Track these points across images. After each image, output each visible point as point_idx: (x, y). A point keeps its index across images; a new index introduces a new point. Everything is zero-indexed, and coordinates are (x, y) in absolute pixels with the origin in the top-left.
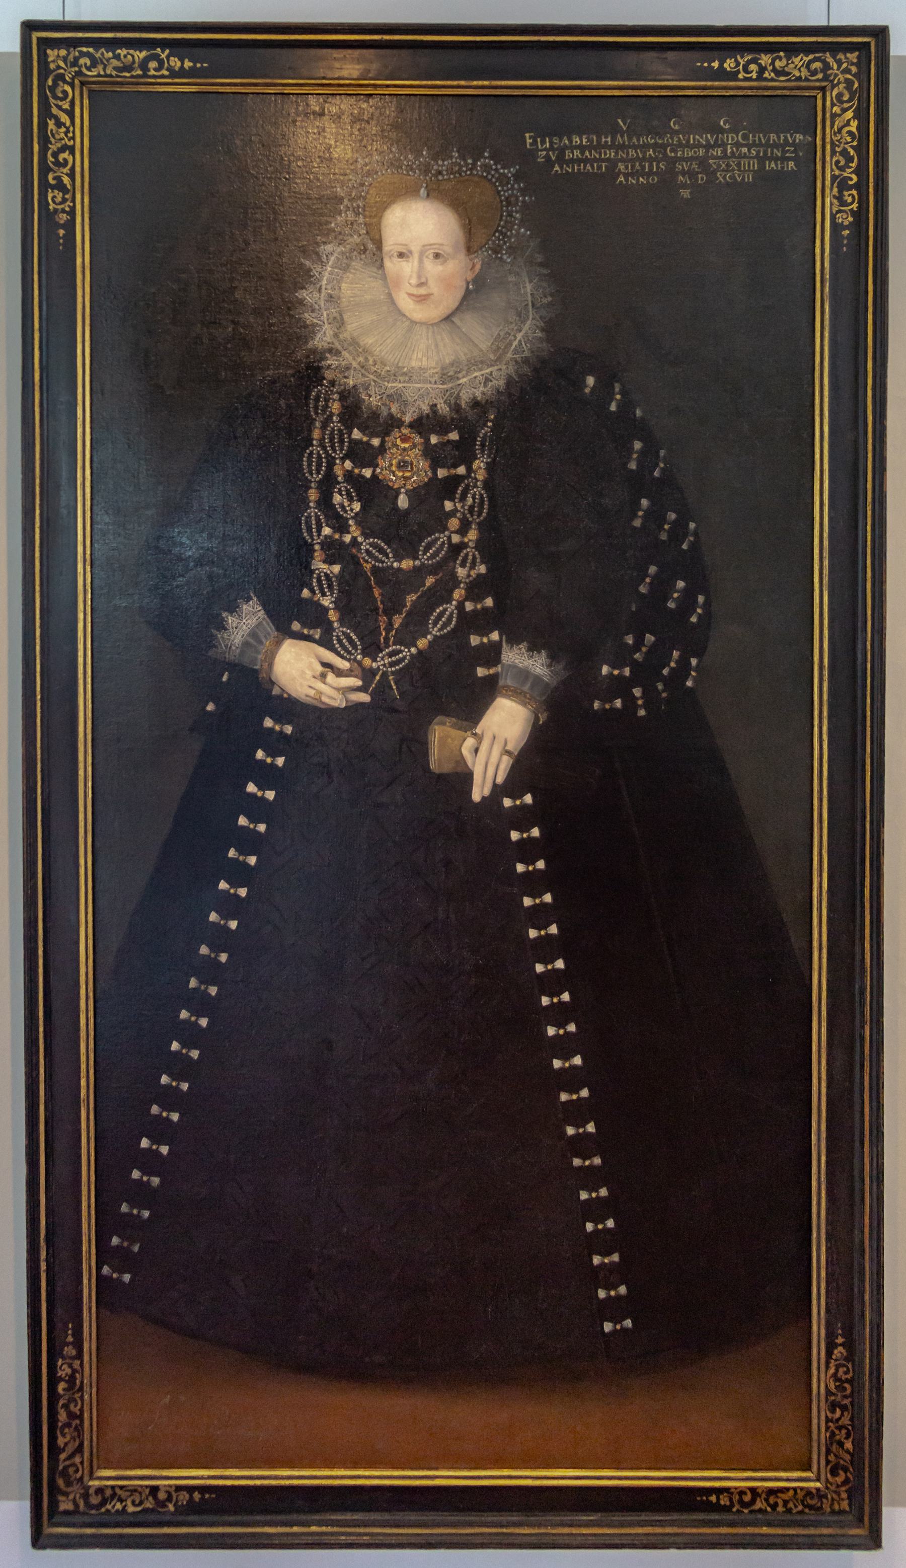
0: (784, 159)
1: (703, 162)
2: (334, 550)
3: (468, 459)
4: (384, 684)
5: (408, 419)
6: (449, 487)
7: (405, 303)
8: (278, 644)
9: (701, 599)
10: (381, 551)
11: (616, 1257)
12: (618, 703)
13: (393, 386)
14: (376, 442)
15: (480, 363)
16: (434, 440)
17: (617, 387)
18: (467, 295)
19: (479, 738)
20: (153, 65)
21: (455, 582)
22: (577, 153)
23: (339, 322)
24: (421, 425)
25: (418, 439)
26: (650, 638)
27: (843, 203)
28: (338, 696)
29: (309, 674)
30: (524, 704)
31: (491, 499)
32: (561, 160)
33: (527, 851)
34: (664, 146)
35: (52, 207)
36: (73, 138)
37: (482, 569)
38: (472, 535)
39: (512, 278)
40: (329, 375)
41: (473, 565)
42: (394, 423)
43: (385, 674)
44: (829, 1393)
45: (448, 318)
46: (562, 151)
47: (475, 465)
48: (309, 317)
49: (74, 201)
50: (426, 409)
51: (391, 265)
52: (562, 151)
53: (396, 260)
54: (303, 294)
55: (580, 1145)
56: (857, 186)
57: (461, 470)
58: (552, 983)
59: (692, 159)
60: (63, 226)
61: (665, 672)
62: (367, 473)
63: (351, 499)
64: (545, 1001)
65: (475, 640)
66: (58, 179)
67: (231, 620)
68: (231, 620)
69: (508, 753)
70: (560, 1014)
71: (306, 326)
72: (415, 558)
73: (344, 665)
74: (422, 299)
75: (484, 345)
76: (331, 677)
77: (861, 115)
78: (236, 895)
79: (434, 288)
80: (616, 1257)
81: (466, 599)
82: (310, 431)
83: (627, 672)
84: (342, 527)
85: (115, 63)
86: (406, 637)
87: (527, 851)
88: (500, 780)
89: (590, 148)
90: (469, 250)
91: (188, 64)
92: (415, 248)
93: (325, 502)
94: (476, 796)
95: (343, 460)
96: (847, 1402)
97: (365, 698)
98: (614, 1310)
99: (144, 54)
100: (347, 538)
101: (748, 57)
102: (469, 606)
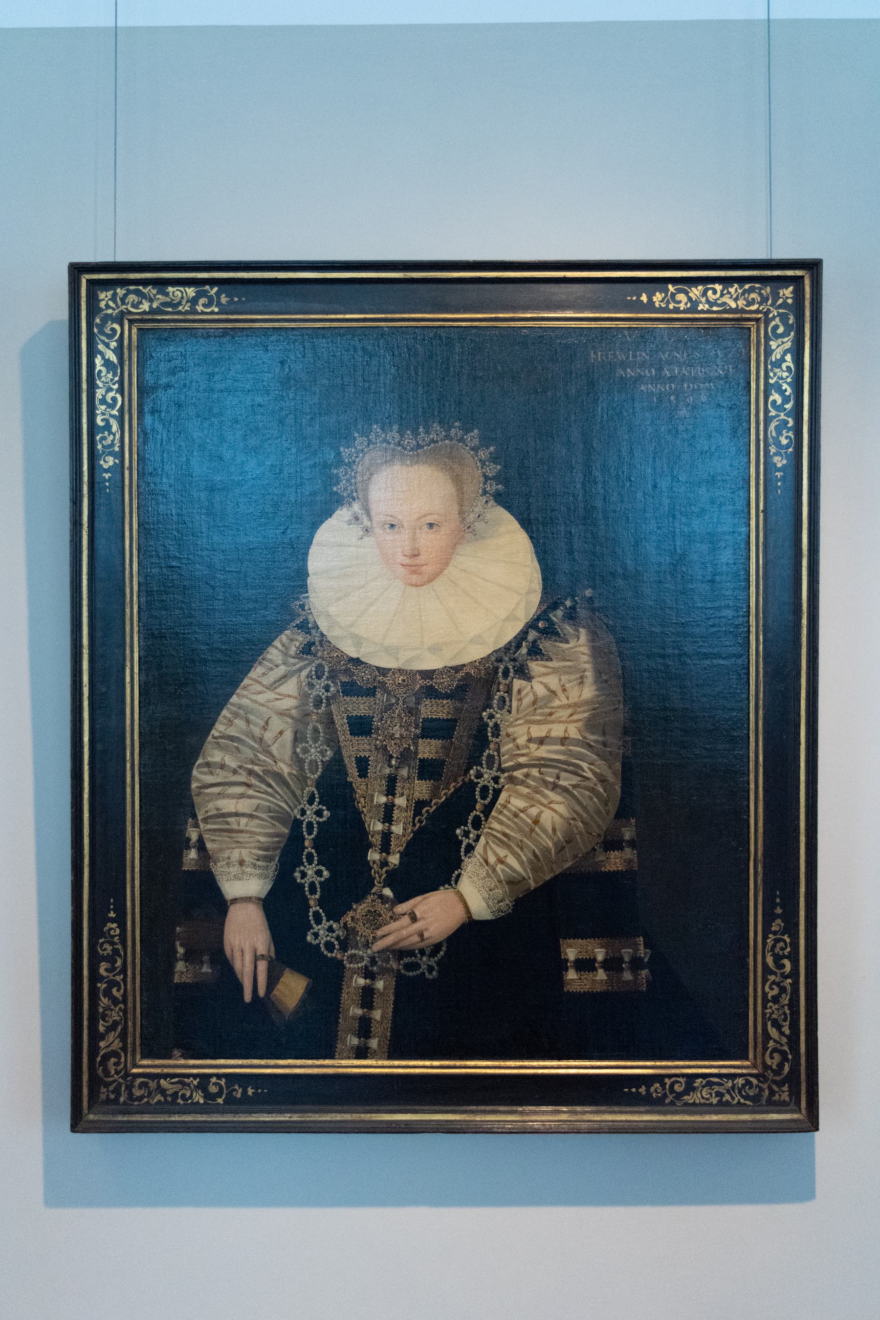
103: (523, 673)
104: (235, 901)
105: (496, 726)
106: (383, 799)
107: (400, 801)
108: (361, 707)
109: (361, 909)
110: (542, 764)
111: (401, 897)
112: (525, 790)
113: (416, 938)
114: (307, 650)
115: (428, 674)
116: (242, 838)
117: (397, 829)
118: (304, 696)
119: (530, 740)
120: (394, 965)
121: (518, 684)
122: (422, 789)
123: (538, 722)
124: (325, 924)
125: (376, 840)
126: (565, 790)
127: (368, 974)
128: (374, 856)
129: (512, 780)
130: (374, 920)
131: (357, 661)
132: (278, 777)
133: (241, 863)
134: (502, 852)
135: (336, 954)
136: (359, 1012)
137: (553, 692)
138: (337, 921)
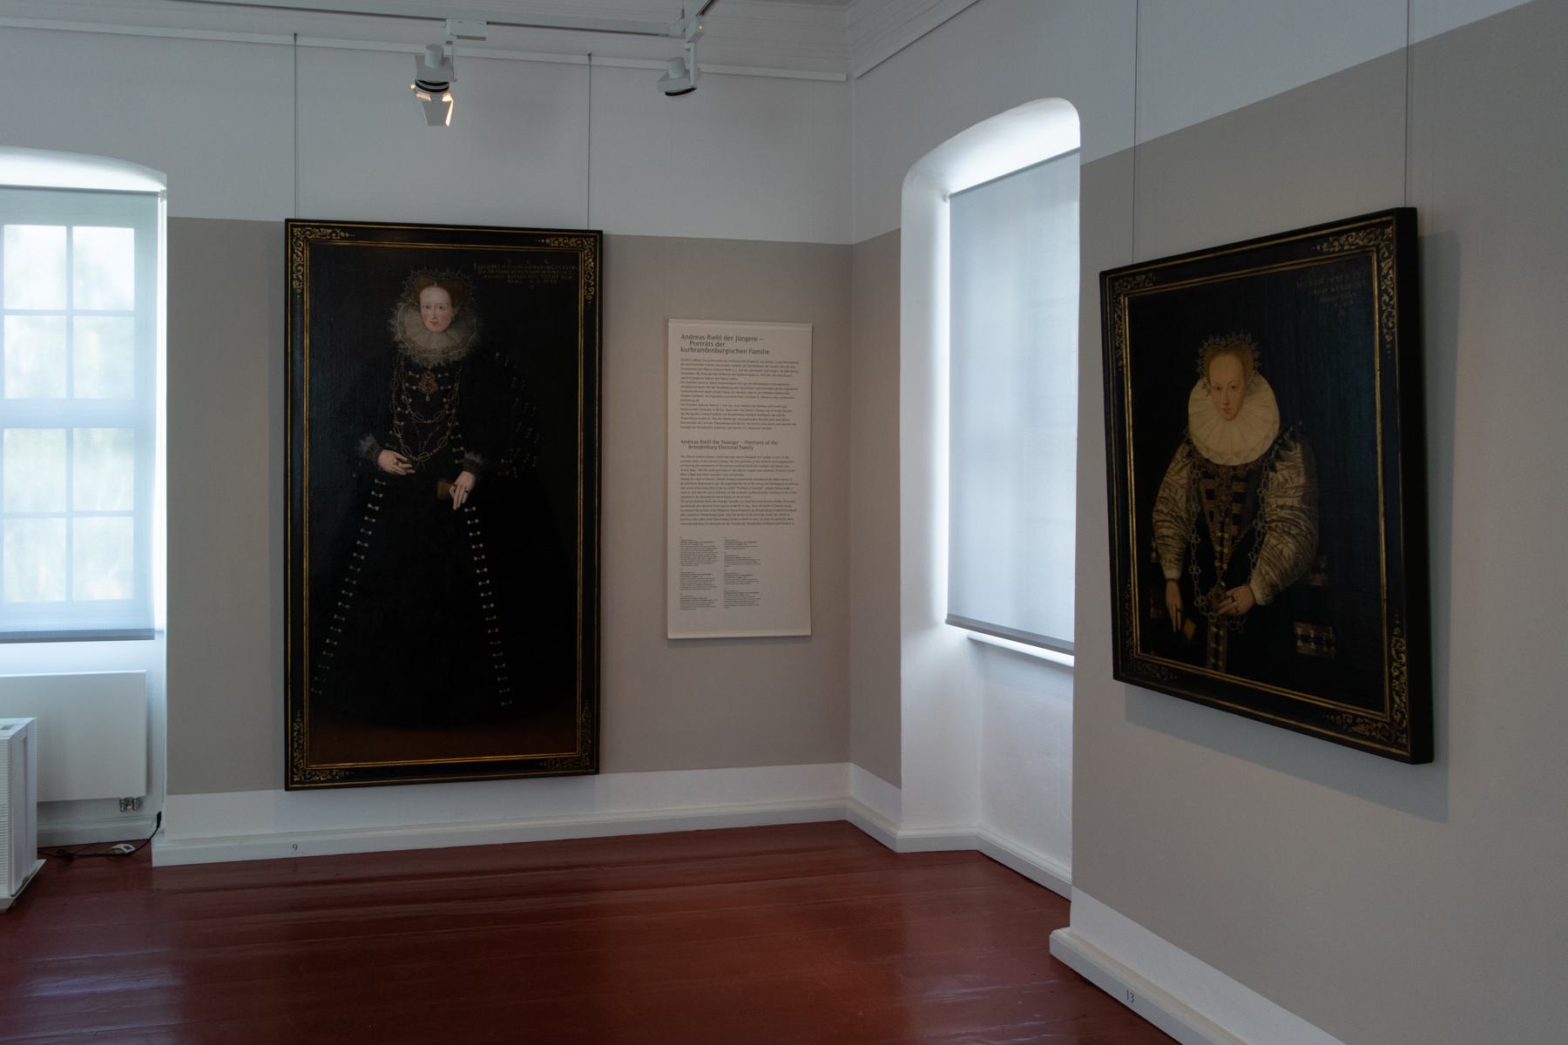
2: (402, 417)
5: (430, 368)
6: (446, 393)
7: (428, 325)
8: (380, 451)
12: (508, 473)
14: (418, 376)
17: (507, 357)
18: (452, 322)
19: (456, 486)
20: (334, 235)
22: (493, 271)
23: (405, 332)
24: (435, 370)
25: (433, 375)
26: (519, 449)
27: (589, 292)
29: (392, 463)
33: (474, 528)
38: (453, 411)
40: (400, 351)
42: (425, 369)
44: (582, 723)
45: (445, 331)
48: (393, 330)
50: (436, 364)
57: (450, 387)
58: (483, 577)
61: (525, 461)
62: (414, 388)
66: (297, 276)
67: (362, 442)
68: (362, 442)
69: (466, 492)
70: (485, 588)
73: (405, 459)
74: (435, 324)
76: (400, 464)
77: (594, 260)
79: (439, 319)
83: (511, 461)
84: (404, 408)
86: (429, 449)
87: (474, 528)
88: (463, 502)
90: (453, 305)
91: (347, 235)
93: (398, 398)
94: (455, 508)
97: (413, 471)
100: (407, 412)
102: (452, 437)
103: (1274, 469)
104: (1169, 580)
105: (1263, 497)
107: (1226, 536)
109: (1213, 591)
110: (1282, 520)
111: (1228, 588)
112: (1276, 535)
114: (1189, 455)
115: (1234, 468)
117: (1226, 551)
118: (1189, 478)
119: (1277, 506)
120: (1226, 623)
121: (1271, 474)
122: (1234, 529)
123: (1281, 497)
124: (1201, 597)
125: (1218, 555)
126: (1294, 536)
127: (1218, 627)
128: (1217, 564)
130: (1219, 598)
131: (1207, 460)
132: (1181, 518)
133: (1170, 561)
134: (1268, 568)
135: (1205, 613)
137: (1286, 480)
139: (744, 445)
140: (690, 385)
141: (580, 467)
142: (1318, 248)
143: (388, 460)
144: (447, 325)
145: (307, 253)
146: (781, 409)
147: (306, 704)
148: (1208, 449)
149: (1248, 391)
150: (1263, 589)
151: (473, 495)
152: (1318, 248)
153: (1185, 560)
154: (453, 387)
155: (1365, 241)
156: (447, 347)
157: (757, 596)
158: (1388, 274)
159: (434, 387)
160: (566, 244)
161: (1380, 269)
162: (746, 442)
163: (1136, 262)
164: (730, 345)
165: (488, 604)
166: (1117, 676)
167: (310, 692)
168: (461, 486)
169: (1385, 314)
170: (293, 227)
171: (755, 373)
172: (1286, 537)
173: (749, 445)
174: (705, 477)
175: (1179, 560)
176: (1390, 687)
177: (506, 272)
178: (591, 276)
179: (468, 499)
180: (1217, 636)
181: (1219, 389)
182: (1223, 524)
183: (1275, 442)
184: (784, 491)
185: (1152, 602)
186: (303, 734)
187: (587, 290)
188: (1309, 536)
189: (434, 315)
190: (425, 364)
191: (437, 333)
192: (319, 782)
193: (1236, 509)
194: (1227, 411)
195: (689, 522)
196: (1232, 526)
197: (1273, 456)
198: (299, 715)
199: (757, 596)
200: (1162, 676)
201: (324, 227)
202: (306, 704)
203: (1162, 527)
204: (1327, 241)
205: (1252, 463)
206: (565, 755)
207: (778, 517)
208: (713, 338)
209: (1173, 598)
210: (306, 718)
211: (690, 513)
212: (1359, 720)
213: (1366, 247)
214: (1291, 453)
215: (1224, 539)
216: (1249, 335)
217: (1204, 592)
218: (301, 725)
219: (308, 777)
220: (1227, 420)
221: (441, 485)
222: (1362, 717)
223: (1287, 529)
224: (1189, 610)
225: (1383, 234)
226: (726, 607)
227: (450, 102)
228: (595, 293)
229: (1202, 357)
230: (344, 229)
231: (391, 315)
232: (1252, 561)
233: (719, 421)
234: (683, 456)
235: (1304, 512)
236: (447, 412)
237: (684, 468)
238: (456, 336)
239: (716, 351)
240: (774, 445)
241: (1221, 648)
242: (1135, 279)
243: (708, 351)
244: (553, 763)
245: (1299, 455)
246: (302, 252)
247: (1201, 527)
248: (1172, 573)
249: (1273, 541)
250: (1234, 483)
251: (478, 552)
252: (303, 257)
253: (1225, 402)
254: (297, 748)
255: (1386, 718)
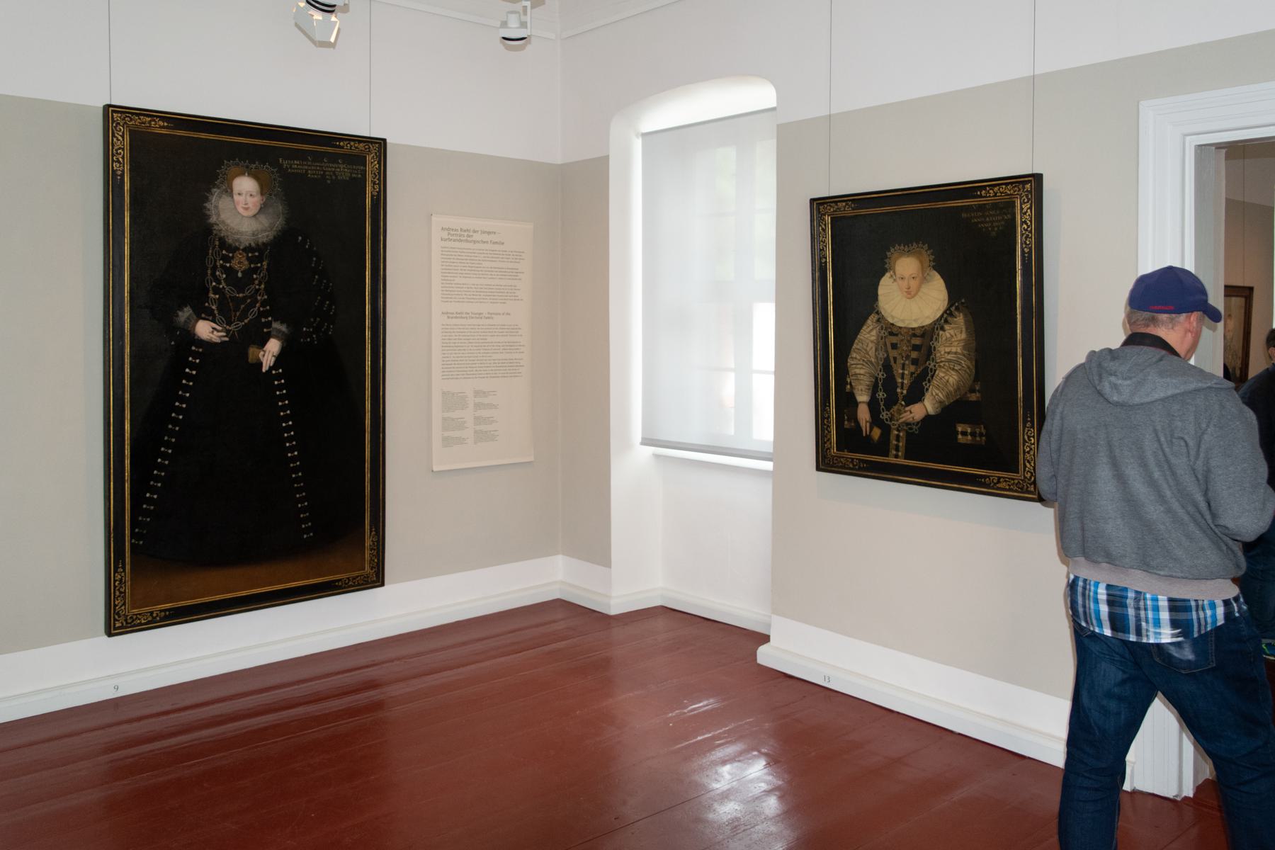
0: (357, 174)
1: (334, 172)
2: (216, 290)
3: (261, 262)
4: (233, 335)
5: (241, 248)
6: (255, 270)
7: (241, 210)
8: (197, 321)
9: (334, 307)
10: (233, 291)
11: (308, 514)
13: (236, 237)
14: (231, 255)
15: (265, 231)
16: (250, 255)
18: (261, 208)
19: (265, 352)
20: (153, 123)
21: (257, 301)
22: (296, 166)
23: (218, 215)
24: (248, 249)
25: (245, 254)
26: (318, 319)
27: (374, 189)
28: (218, 339)
29: (208, 331)
30: (279, 340)
31: (269, 275)
32: (291, 167)
33: (280, 387)
34: (322, 167)
35: (115, 168)
36: (124, 145)
37: (266, 297)
38: (263, 286)
39: (275, 204)
40: (215, 232)
41: (263, 296)
42: (237, 249)
43: (234, 332)
44: (370, 546)
45: (255, 216)
46: (291, 165)
47: (264, 263)
48: (208, 212)
49: (124, 167)
50: (247, 245)
51: (236, 197)
52: (291, 165)
53: (238, 196)
54: (206, 205)
55: (297, 480)
56: (378, 184)
57: (259, 265)
58: (288, 429)
59: (331, 171)
60: (120, 176)
61: (323, 329)
62: (228, 265)
63: (222, 274)
64: (286, 435)
65: (263, 320)
66: (118, 159)
67: (180, 313)
68: (180, 313)
69: (274, 356)
71: (207, 215)
72: (244, 293)
74: (246, 209)
75: (267, 225)
76: (215, 333)
77: (379, 163)
78: (182, 407)
79: (250, 205)
80: (308, 514)
81: (261, 306)
82: (208, 250)
85: (139, 120)
88: (271, 365)
89: (300, 165)
90: (262, 194)
91: (166, 124)
92: (244, 192)
93: (213, 274)
94: (264, 370)
95: (220, 260)
96: (375, 548)
97: (227, 339)
98: (307, 530)
99: (150, 119)
100: (221, 286)
101: (348, 142)
102: (261, 309)
103: (943, 329)
104: (860, 402)
105: (934, 347)
106: (901, 371)
107: (906, 372)
108: (894, 340)
109: (895, 408)
110: (949, 361)
111: (907, 405)
112: (944, 370)
113: (911, 419)
114: (878, 320)
115: (913, 329)
116: (862, 382)
117: (905, 382)
118: (878, 336)
119: (945, 352)
120: (905, 428)
121: (941, 332)
122: (912, 368)
123: (947, 346)
124: (885, 412)
125: (899, 385)
126: (956, 370)
127: (898, 430)
128: (899, 390)
129: (940, 366)
130: (899, 412)
131: (893, 324)
132: (871, 362)
133: (862, 390)
134: (937, 392)
135: (889, 423)
136: (896, 443)
137: (952, 336)
138: (889, 411)
139: (487, 316)
140: (447, 268)
141: (368, 334)
142: (979, 193)
143: (205, 330)
144: (257, 211)
145: (127, 137)
146: (513, 288)
147: (128, 554)
148: (893, 317)
149: (924, 280)
150: (934, 404)
151: (280, 359)
152: (979, 193)
153: (874, 389)
154: (262, 265)
155: (1012, 191)
156: (257, 230)
157: (496, 433)
158: (1027, 212)
159: (246, 264)
160: (356, 148)
161: (1022, 209)
162: (489, 313)
163: (831, 195)
164: (477, 237)
165: (292, 452)
166: (818, 469)
167: (131, 543)
168: (270, 351)
169: (1025, 236)
170: (110, 112)
171: (494, 259)
172: (951, 371)
173: (490, 316)
174: (460, 341)
175: (869, 389)
176: (1024, 457)
177: (306, 167)
178: (376, 176)
179: (275, 362)
180: (898, 436)
181: (902, 278)
182: (904, 365)
183: (945, 312)
184: (515, 351)
185: (846, 417)
186: (125, 582)
187: (374, 187)
188: (968, 370)
189: (246, 201)
190: (237, 244)
191: (247, 217)
192: (141, 624)
193: (914, 355)
194: (909, 293)
195: (448, 377)
196: (911, 366)
197: (943, 321)
198: (120, 566)
199: (496, 433)
200: (854, 465)
201: (144, 115)
202: (128, 554)
203: (856, 368)
204: (985, 190)
205: (927, 326)
206: (356, 574)
207: (512, 371)
208: (465, 231)
209: (864, 414)
210: (128, 567)
211: (449, 370)
212: (1002, 480)
213: (1012, 195)
214: (955, 319)
215: (904, 376)
216: (927, 245)
217: (888, 409)
218: (123, 574)
219: (129, 621)
220: (909, 298)
221: (252, 351)
222: (1004, 478)
223: (952, 367)
224: (876, 420)
225: (1024, 188)
226: (475, 443)
227: (337, 22)
228: (380, 189)
229: (890, 258)
230: (162, 119)
231: (206, 199)
232: (926, 387)
233: (469, 297)
234: (443, 325)
235: (964, 355)
236: (257, 287)
237: (444, 334)
238: (265, 221)
239: (467, 241)
240: (508, 316)
241: (901, 444)
242: (837, 205)
243: (461, 241)
244: (347, 582)
245: (963, 321)
246: (123, 137)
247: (887, 367)
248: (863, 397)
249: (942, 375)
250: (914, 338)
251: (284, 408)
252: (123, 141)
253: (907, 287)
254: (119, 596)
255: (1021, 476)
